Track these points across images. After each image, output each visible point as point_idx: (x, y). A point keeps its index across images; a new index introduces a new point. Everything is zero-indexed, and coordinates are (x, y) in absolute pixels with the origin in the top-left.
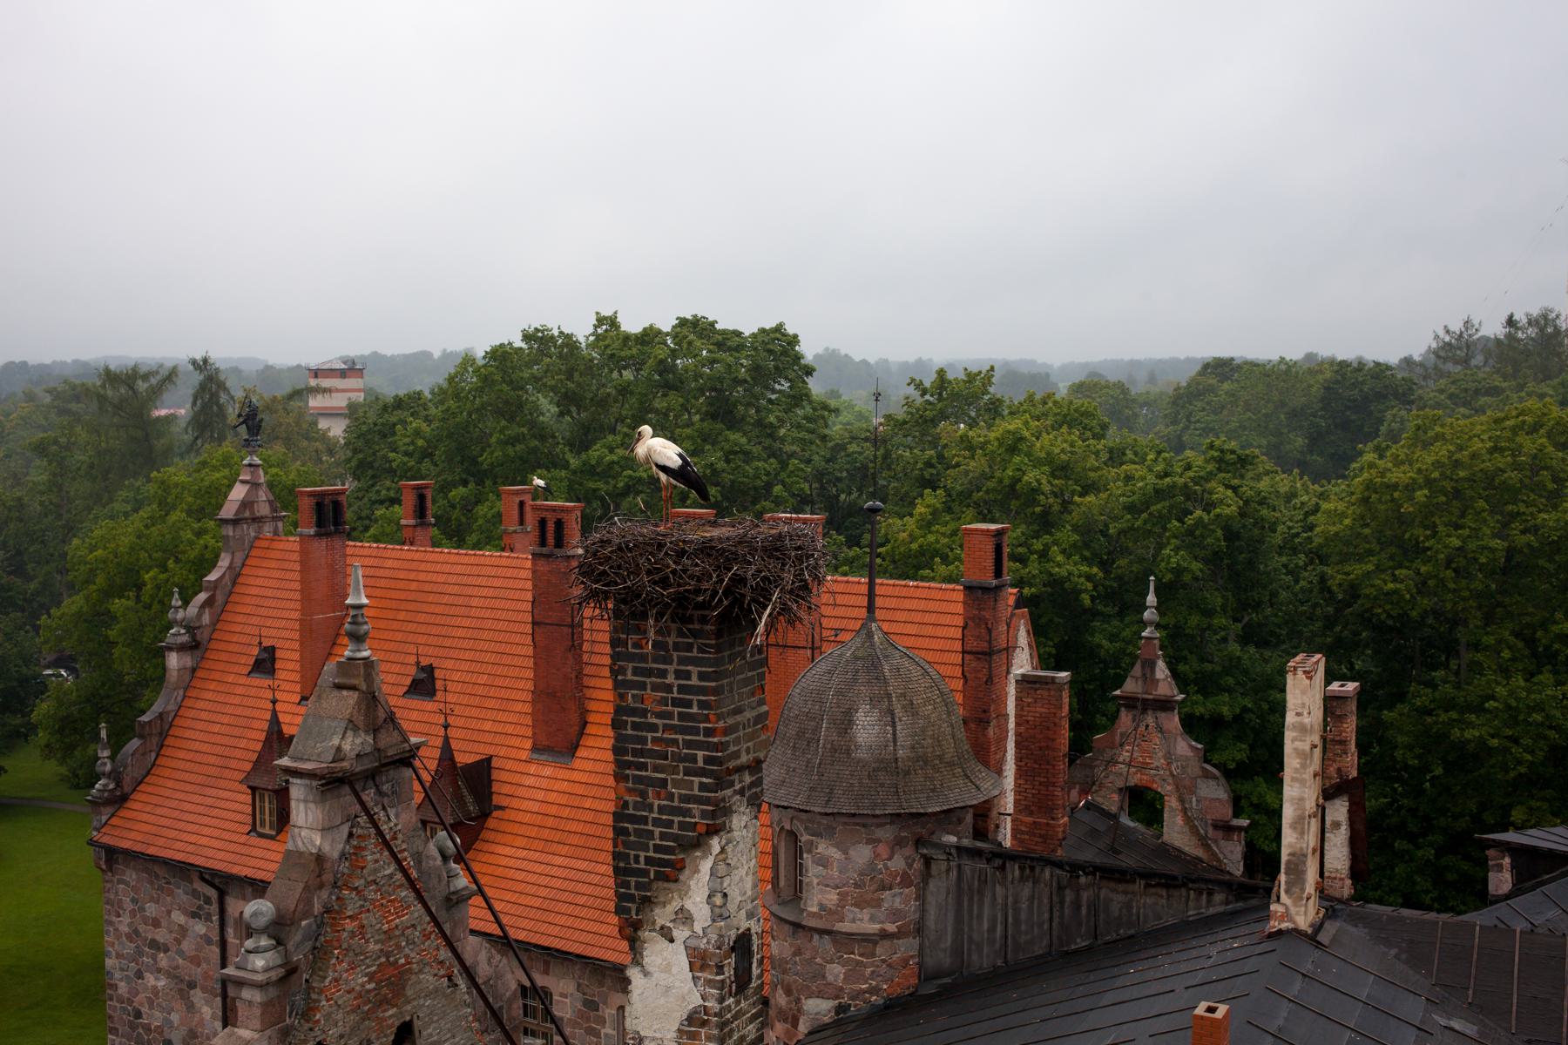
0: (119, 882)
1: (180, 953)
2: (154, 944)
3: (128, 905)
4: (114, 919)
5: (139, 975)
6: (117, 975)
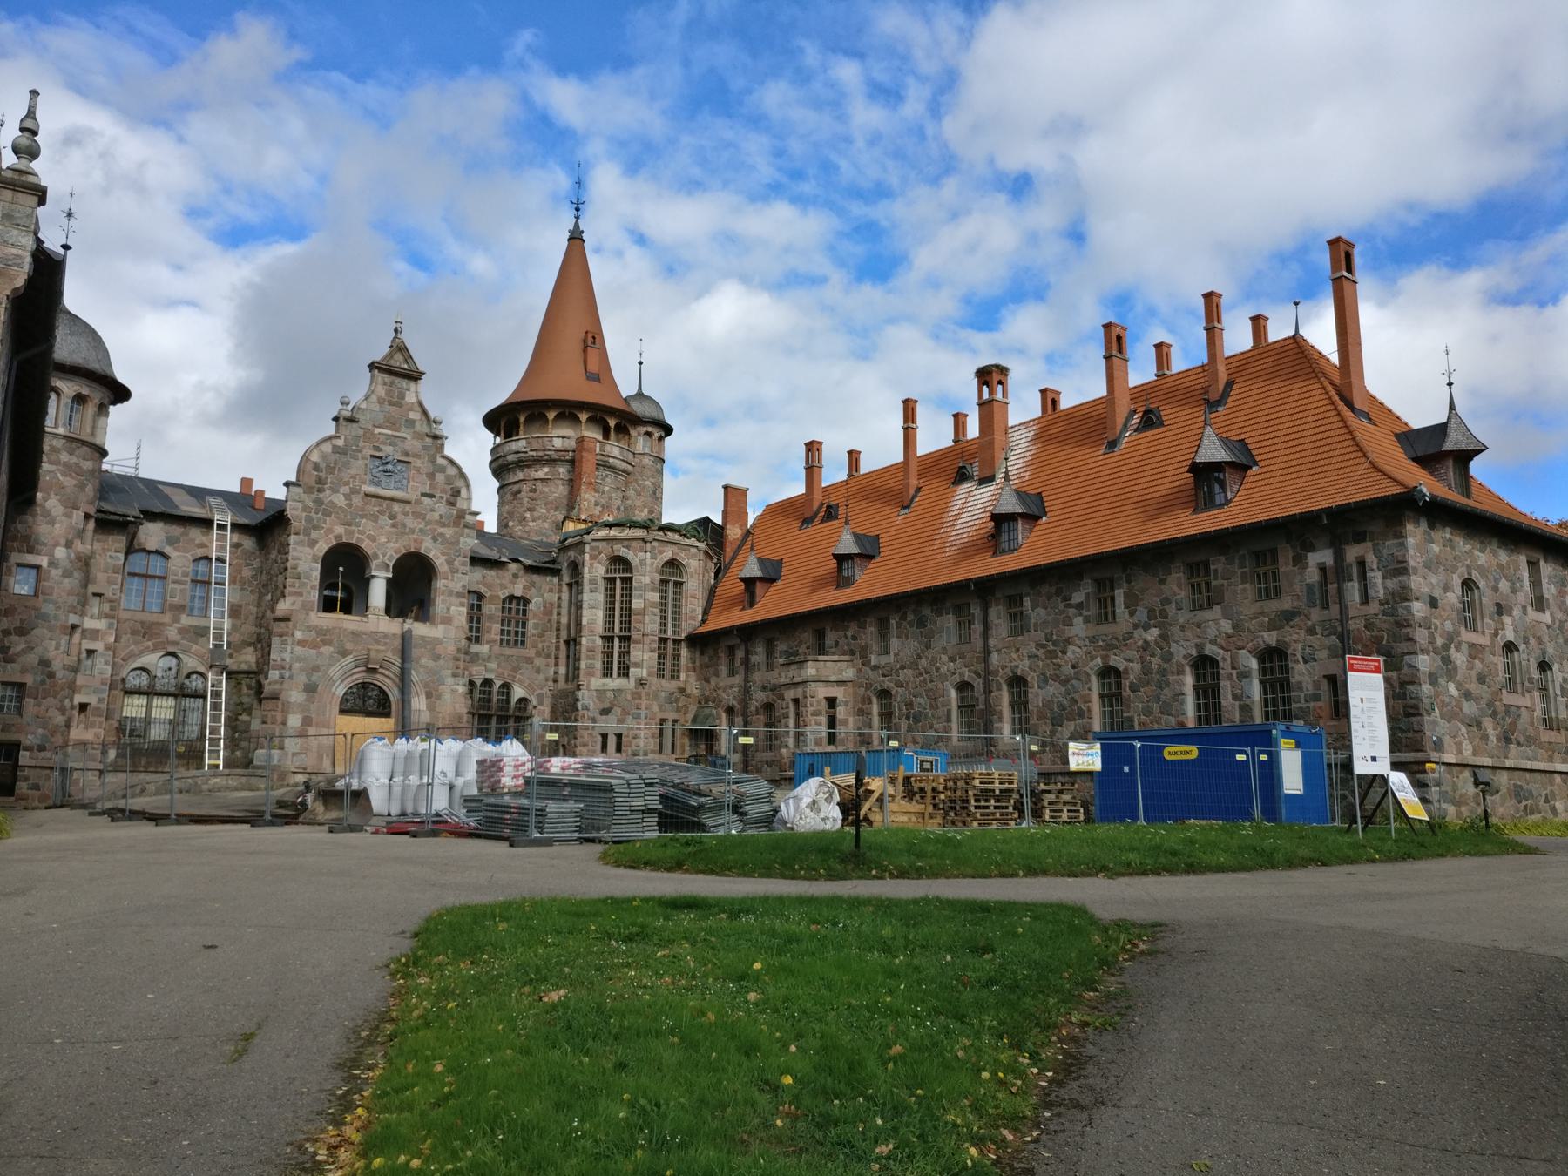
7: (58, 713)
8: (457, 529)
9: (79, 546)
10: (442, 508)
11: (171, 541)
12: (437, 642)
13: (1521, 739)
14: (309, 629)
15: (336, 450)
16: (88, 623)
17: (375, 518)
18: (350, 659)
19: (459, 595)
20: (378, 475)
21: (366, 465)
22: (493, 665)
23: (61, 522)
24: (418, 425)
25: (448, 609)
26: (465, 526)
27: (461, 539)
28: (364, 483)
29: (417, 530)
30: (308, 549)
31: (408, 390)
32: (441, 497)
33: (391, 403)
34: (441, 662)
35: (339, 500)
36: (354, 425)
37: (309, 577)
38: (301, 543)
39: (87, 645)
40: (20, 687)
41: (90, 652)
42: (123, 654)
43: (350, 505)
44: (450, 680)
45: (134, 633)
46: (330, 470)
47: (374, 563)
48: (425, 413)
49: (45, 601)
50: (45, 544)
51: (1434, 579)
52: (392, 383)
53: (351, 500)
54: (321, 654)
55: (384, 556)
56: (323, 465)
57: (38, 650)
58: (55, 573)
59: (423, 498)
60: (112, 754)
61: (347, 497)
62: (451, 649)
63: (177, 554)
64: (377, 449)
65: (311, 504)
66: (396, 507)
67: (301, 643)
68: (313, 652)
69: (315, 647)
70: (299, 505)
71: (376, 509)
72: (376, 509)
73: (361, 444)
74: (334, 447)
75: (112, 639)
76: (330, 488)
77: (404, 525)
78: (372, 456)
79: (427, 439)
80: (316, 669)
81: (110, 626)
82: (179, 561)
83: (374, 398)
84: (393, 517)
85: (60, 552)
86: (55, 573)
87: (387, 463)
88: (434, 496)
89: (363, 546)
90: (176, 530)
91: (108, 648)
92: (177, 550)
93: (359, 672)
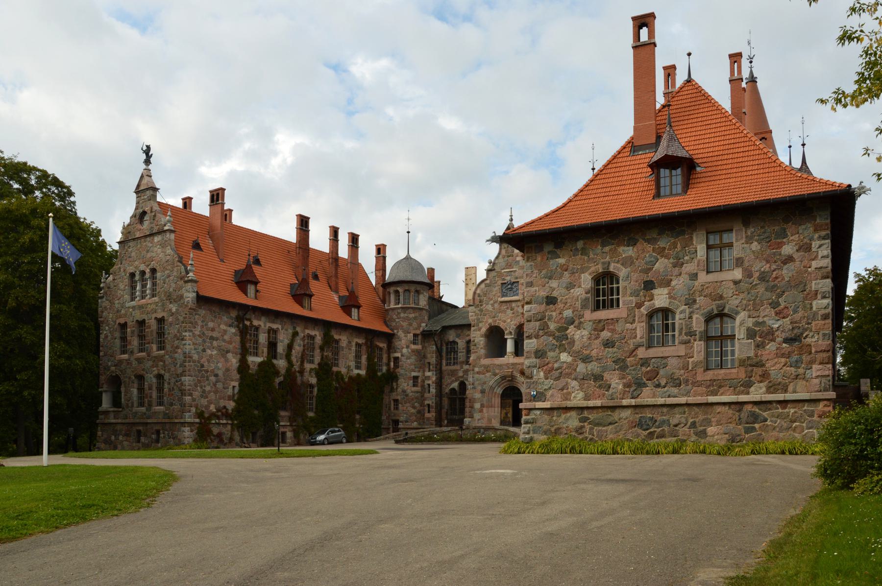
1: (224, 341)
2: (212, 338)
3: (200, 323)
4: (193, 329)
5: (204, 350)
7: (411, 409)
9: (413, 347)
11: (458, 336)
13: (663, 382)
15: (487, 286)
16: (428, 374)
17: (504, 312)
18: (498, 377)
24: (521, 262)
28: (499, 297)
30: (478, 332)
35: (490, 307)
36: (493, 272)
37: (479, 345)
40: (396, 401)
41: (429, 385)
42: (446, 384)
43: (494, 309)
45: (448, 375)
47: (506, 332)
51: (554, 284)
54: (485, 376)
56: (481, 294)
57: (401, 387)
58: (403, 358)
60: (446, 422)
61: (493, 305)
64: (504, 279)
66: (514, 305)
67: (478, 373)
74: (485, 284)
75: (434, 379)
76: (485, 303)
77: (518, 312)
78: (502, 284)
80: (485, 383)
85: (405, 351)
86: (403, 359)
90: (459, 331)
91: (433, 383)
92: (460, 339)
93: (505, 382)
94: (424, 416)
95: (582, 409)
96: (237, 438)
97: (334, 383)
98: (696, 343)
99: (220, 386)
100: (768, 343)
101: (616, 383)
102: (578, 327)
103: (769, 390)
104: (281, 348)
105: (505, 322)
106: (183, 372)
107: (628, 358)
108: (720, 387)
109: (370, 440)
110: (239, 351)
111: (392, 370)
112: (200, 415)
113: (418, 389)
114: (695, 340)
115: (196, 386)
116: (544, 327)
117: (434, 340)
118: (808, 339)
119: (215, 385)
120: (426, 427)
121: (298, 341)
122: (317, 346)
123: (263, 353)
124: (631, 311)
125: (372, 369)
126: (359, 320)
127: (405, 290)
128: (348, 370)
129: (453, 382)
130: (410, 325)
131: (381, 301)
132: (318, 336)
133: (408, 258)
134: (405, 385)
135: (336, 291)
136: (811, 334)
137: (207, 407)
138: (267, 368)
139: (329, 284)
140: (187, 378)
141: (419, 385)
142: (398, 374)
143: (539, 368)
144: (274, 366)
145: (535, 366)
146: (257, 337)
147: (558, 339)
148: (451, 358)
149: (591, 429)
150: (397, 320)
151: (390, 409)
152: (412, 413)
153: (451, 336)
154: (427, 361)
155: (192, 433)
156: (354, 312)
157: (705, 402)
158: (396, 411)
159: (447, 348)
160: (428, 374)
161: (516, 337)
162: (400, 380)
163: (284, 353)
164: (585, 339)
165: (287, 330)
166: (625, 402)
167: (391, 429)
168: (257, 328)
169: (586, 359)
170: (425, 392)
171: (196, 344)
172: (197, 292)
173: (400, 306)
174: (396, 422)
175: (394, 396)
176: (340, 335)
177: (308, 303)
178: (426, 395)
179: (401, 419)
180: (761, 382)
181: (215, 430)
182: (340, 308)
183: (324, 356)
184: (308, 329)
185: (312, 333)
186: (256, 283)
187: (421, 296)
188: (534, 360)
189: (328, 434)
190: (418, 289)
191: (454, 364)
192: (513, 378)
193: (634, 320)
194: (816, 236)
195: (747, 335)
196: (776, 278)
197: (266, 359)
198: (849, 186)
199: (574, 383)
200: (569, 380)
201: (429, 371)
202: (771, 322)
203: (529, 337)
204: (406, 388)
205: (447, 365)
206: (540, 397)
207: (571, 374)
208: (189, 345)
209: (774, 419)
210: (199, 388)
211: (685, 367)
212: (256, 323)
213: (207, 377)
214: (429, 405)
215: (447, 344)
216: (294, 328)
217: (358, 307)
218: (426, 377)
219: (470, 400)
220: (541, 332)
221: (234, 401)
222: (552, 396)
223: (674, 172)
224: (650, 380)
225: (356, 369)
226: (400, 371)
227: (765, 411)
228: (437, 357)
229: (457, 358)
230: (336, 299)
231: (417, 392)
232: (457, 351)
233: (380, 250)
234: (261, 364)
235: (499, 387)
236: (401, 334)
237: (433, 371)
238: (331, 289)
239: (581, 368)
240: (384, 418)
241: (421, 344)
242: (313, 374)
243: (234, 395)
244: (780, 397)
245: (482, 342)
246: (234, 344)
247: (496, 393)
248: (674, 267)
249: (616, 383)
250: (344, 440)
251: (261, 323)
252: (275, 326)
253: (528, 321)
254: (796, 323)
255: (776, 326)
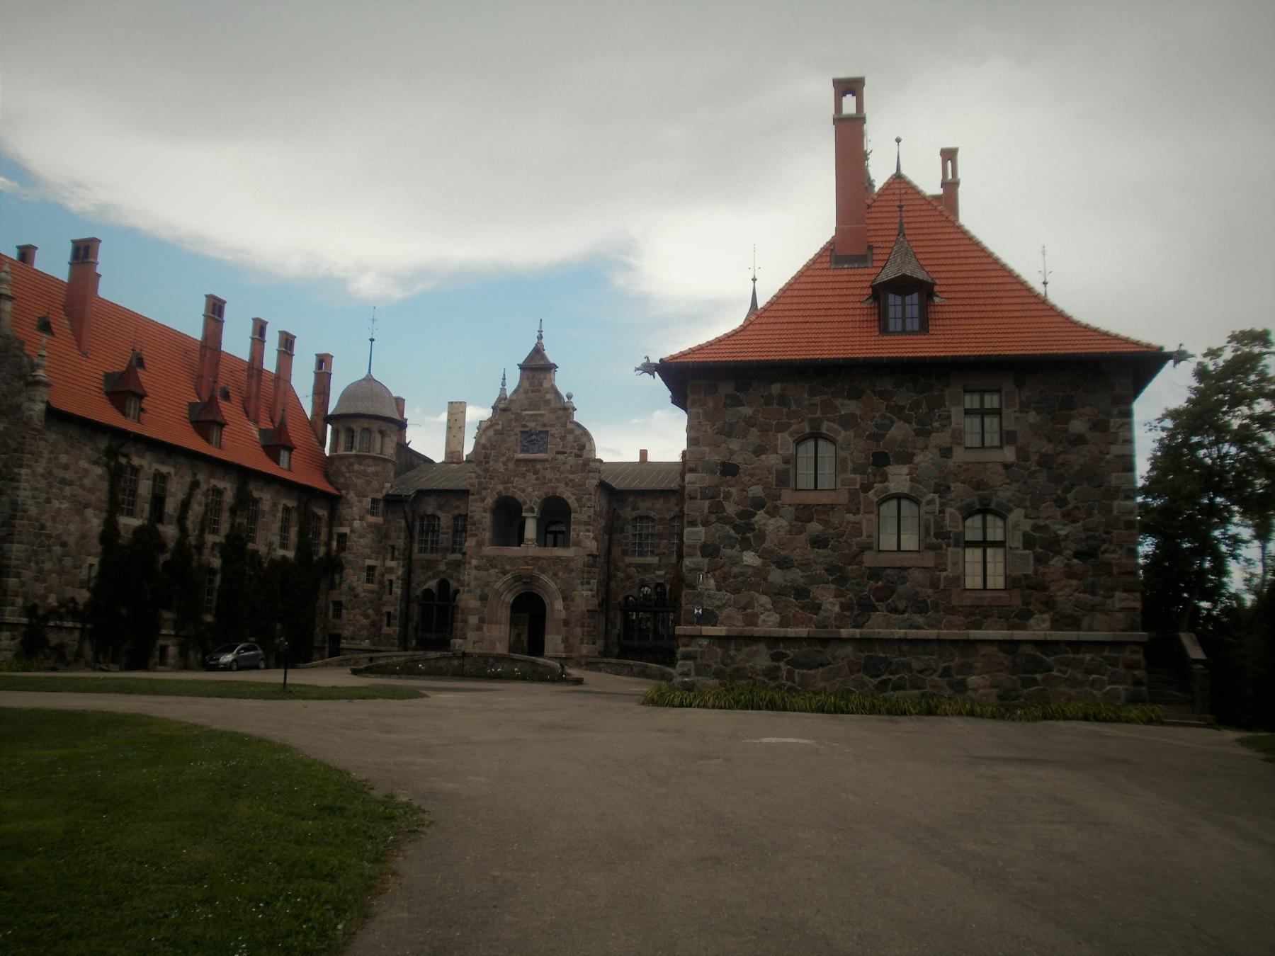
0: (42, 439)
1: (82, 487)
2: (64, 482)
3: (46, 455)
4: (33, 463)
5: (48, 501)
6: (30, 502)
7: (362, 618)
8: (583, 475)
9: (371, 519)
10: (571, 460)
11: (440, 507)
12: (569, 560)
13: (902, 605)
14: (482, 557)
15: (497, 432)
16: (390, 563)
17: (523, 476)
18: (509, 576)
19: (587, 524)
20: (527, 444)
21: (517, 439)
22: (662, 573)
23: (356, 506)
25: (578, 535)
26: (590, 471)
27: (587, 481)
28: (516, 452)
29: (554, 480)
30: (481, 505)
31: (545, 379)
32: (571, 453)
33: (533, 391)
34: (573, 574)
35: (500, 467)
38: (476, 500)
39: (388, 577)
40: (338, 605)
41: (391, 582)
43: (506, 469)
44: (580, 587)
46: (493, 447)
47: (525, 507)
48: (557, 393)
49: (351, 553)
50: (347, 520)
51: (734, 444)
52: (534, 377)
53: (507, 465)
55: (531, 501)
57: (348, 581)
58: (353, 535)
59: (557, 456)
60: (414, 643)
61: (505, 463)
62: (580, 565)
63: (443, 515)
64: (525, 426)
65: (482, 473)
66: (539, 466)
67: (477, 568)
68: (485, 573)
69: (486, 570)
70: (474, 475)
71: (524, 469)
72: (524, 469)
73: (514, 424)
74: (495, 431)
75: (400, 572)
76: (494, 460)
77: (544, 478)
78: (522, 432)
79: (559, 412)
80: (487, 584)
81: (398, 564)
82: (445, 519)
83: (521, 391)
84: (536, 473)
86: (354, 537)
87: (532, 435)
88: (566, 453)
89: (516, 497)
91: (398, 578)
94: (380, 631)
95: (772, 641)
96: (88, 652)
97: (247, 569)
98: (950, 549)
99: (68, 562)
100: (1053, 557)
101: (830, 603)
102: (773, 513)
103: (1056, 625)
104: (171, 507)
105: (523, 491)
106: (8, 535)
107: (849, 565)
108: (986, 617)
109: (301, 665)
110: (106, 506)
111: (333, 554)
112: (30, 611)
113: (374, 587)
114: (948, 545)
115: (29, 561)
116: (717, 508)
117: (404, 511)
118: (1107, 555)
119: (60, 560)
120: (383, 649)
121: (199, 496)
122: (226, 507)
123: (143, 511)
124: (853, 495)
125: (305, 548)
126: (289, 469)
127: (364, 429)
128: (269, 549)
129: (427, 580)
130: (368, 483)
131: (320, 442)
132: (229, 490)
133: (369, 379)
134: (354, 579)
135: (256, 422)
136: (1112, 548)
137: (44, 598)
138: (147, 536)
139: (244, 408)
140: (16, 547)
141: (376, 580)
142: (343, 560)
143: (708, 572)
144: (157, 534)
145: (700, 570)
146: (135, 485)
147: (737, 528)
148: (427, 541)
149: (790, 672)
150: (347, 475)
151: (326, 616)
152: (362, 625)
153: (430, 507)
154: (391, 543)
155: (12, 642)
156: (284, 455)
157: (965, 638)
158: (337, 621)
159: (422, 525)
160: (390, 563)
161: (538, 516)
162: (346, 571)
163: (176, 515)
164: (782, 533)
165: (182, 477)
166: (845, 632)
167: (327, 650)
168: (136, 471)
169: (784, 564)
170: (384, 592)
171: (36, 489)
172: (48, 403)
173: (354, 452)
174: (336, 639)
175: (335, 595)
176: (262, 491)
177: (217, 436)
178: (386, 597)
179: (346, 633)
180: (1042, 612)
181: (54, 639)
182: (261, 449)
183: (236, 525)
184: (215, 479)
185: (221, 485)
186: (141, 396)
187: (387, 440)
188: (700, 559)
189: (238, 653)
190: (383, 429)
191: (432, 552)
192: (533, 579)
193: (858, 509)
194: (1115, 411)
195: (1024, 542)
196: (1063, 465)
197: (146, 522)
198: (1161, 348)
199: (764, 599)
200: (756, 595)
201: (393, 559)
202: (1058, 527)
203: (692, 524)
204: (355, 584)
205: (420, 552)
206: (709, 617)
207: (759, 585)
208: (25, 489)
209: (1063, 668)
210: (32, 564)
211: (934, 584)
212: (136, 461)
213: (49, 546)
214: (389, 614)
215: (422, 519)
216: (195, 475)
217: (290, 449)
218: (386, 568)
219: (463, 610)
220: (713, 518)
221: (89, 589)
222: (728, 617)
223: (908, 299)
224: (882, 601)
225: (280, 548)
226: (347, 556)
227: (1048, 656)
228: (405, 539)
229: (437, 541)
230: (256, 433)
231: (373, 592)
232: (438, 531)
233: (323, 361)
234: (138, 531)
235: (509, 592)
236: (352, 496)
237: (398, 559)
238: (248, 417)
239: (776, 576)
240: (318, 630)
241: (383, 516)
242: (216, 552)
243: (89, 581)
244: (1071, 635)
245: (484, 520)
246: (98, 494)
247: (504, 601)
248: (917, 435)
249: (830, 603)
250: (262, 666)
251: (144, 463)
252: (165, 469)
253: (691, 498)
254: (1092, 531)
255: (1063, 533)
